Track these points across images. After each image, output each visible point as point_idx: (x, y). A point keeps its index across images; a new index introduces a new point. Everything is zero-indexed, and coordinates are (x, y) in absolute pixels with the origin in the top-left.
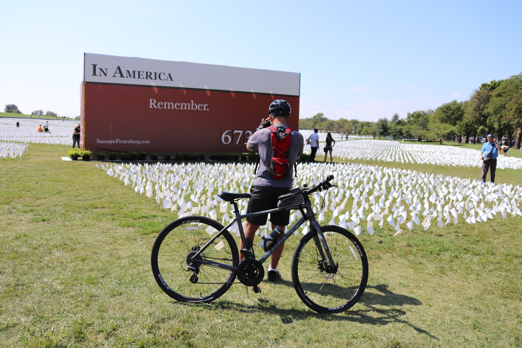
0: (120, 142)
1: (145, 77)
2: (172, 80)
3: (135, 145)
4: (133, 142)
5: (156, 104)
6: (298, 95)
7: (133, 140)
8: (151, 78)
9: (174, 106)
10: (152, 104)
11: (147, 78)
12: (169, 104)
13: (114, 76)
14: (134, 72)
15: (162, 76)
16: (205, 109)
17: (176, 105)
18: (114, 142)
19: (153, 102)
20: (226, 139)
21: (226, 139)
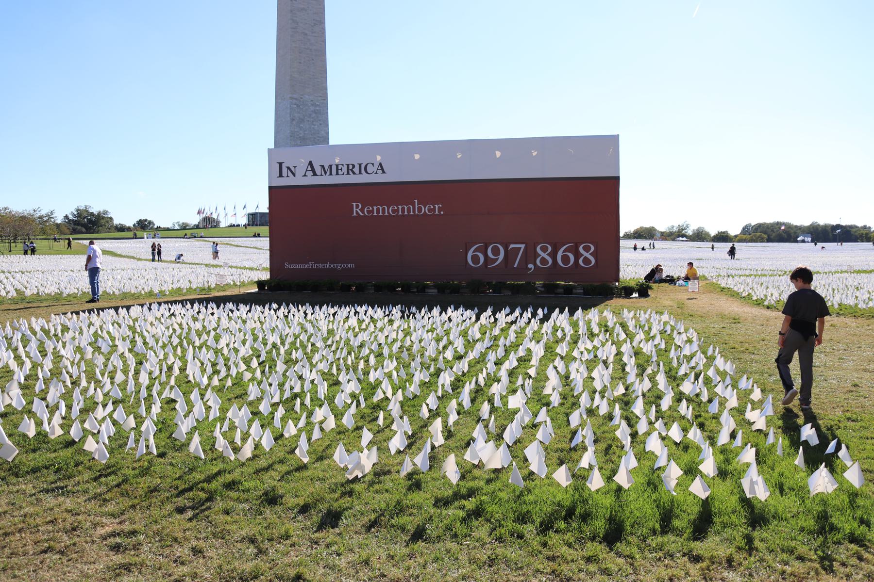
0: (315, 266)
2: (384, 172)
3: (334, 269)
5: (362, 210)
8: (354, 173)
9: (389, 211)
11: (348, 173)
13: (305, 175)
14: (330, 166)
15: (370, 169)
18: (306, 266)
19: (357, 207)
20: (475, 259)
21: (475, 259)
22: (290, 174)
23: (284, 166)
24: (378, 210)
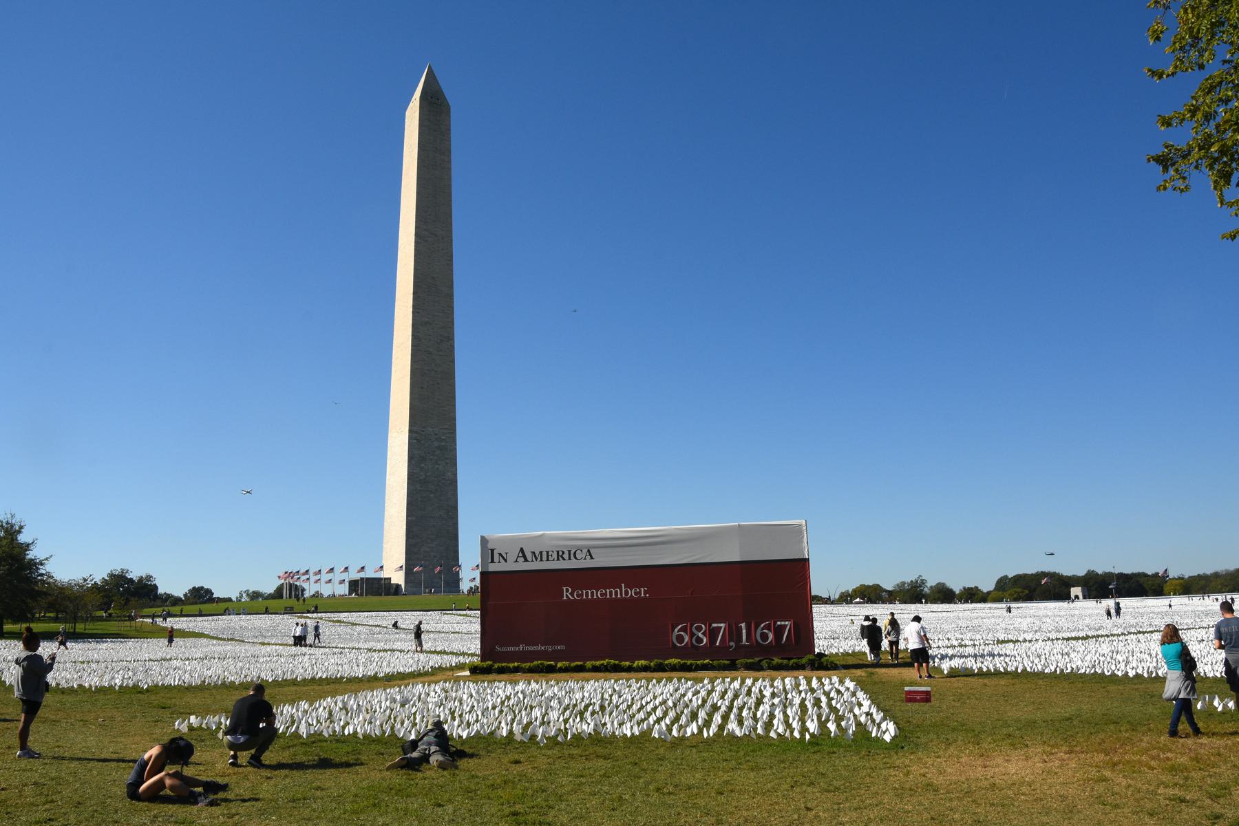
5: (572, 594)
9: (598, 594)
10: (567, 593)
21: (680, 639)
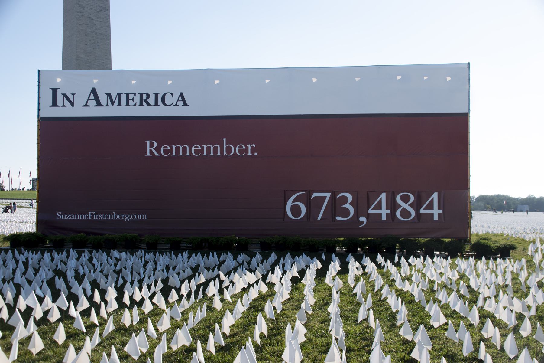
0: (96, 217)
1: (138, 104)
2: (185, 104)
3: (122, 221)
4: (118, 217)
6: (465, 111)
7: (117, 213)
8: (148, 104)
9: (191, 151)
11: (141, 105)
12: (181, 148)
13: (86, 105)
14: (119, 95)
15: (168, 99)
16: (249, 154)
17: (193, 148)
18: (84, 217)
19: (152, 145)
20: (296, 210)
21: (296, 210)
22: (67, 103)
23: (59, 93)
24: (178, 150)
